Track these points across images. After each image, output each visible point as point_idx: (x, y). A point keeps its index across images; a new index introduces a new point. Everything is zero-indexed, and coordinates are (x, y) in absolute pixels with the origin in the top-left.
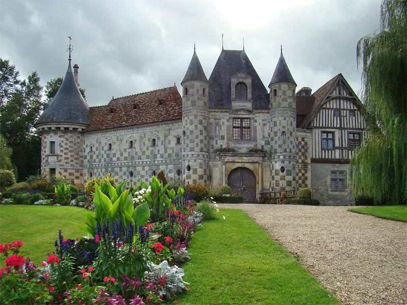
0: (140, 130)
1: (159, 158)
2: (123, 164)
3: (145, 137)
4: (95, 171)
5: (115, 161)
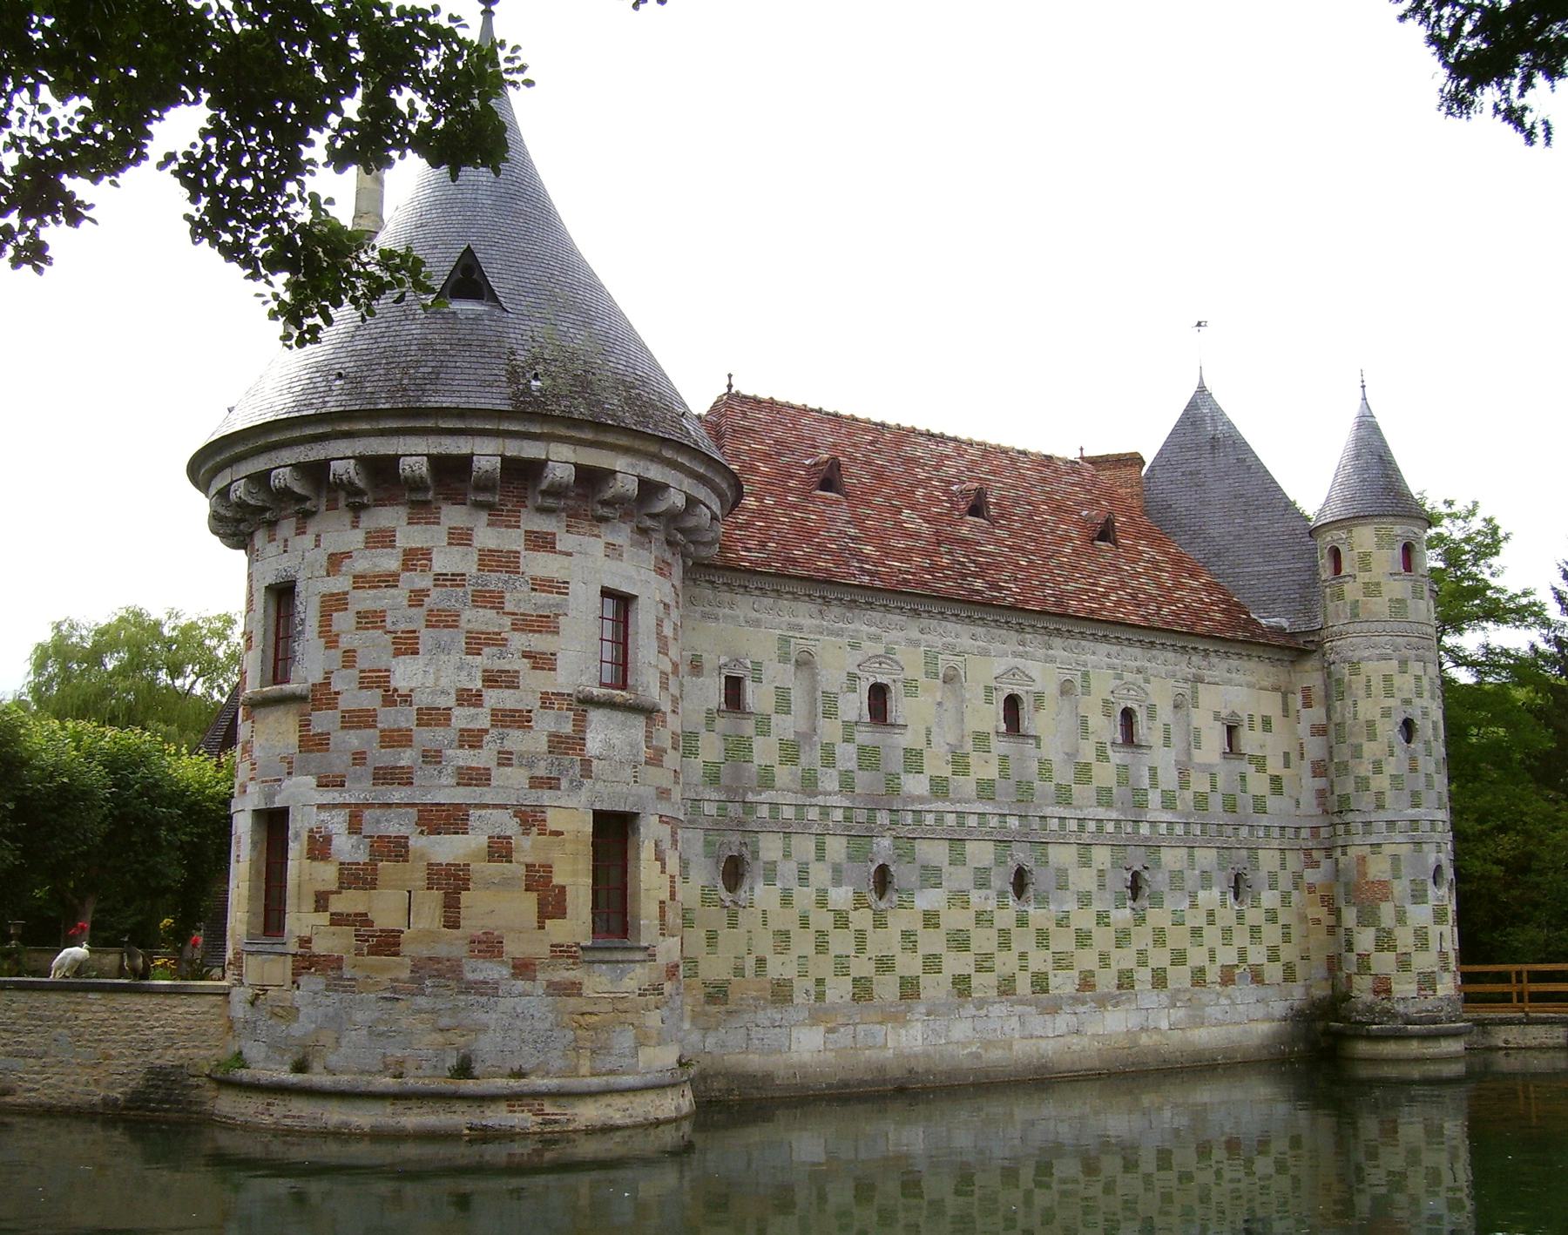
0: (1060, 649)
1: (1155, 811)
2: (972, 821)
3: (1087, 690)
4: (770, 848)
5: (921, 800)
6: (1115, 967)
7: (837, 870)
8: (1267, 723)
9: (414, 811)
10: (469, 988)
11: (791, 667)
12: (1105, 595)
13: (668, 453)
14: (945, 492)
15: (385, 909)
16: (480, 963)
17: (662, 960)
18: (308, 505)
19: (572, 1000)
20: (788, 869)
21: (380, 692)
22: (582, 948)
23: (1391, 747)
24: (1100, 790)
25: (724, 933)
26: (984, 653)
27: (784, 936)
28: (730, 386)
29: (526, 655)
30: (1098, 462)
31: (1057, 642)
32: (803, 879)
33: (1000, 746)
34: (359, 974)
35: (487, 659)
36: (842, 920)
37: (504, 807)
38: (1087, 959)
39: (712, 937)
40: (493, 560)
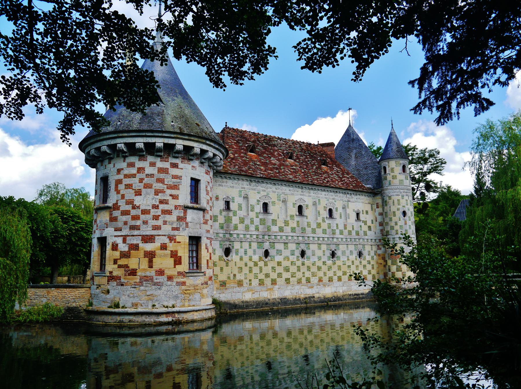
1: (338, 235)
4: (237, 245)
6: (328, 276)
7: (254, 251)
8: (367, 212)
9: (140, 237)
10: (156, 284)
11: (242, 198)
12: (324, 179)
13: (208, 142)
14: (283, 153)
15: (133, 263)
16: (158, 277)
17: (207, 275)
18: (111, 156)
19: (183, 287)
20: (241, 252)
21: (131, 205)
22: (186, 273)
23: (400, 218)
24: (323, 230)
25: (225, 268)
26: (293, 194)
27: (241, 269)
28: (226, 126)
29: (171, 195)
30: (323, 145)
31: (312, 191)
32: (246, 252)
33: (297, 219)
34: (126, 281)
35: (161, 196)
36: (256, 264)
37: (165, 235)
38: (320, 274)
39: (222, 269)
40: (161, 170)
